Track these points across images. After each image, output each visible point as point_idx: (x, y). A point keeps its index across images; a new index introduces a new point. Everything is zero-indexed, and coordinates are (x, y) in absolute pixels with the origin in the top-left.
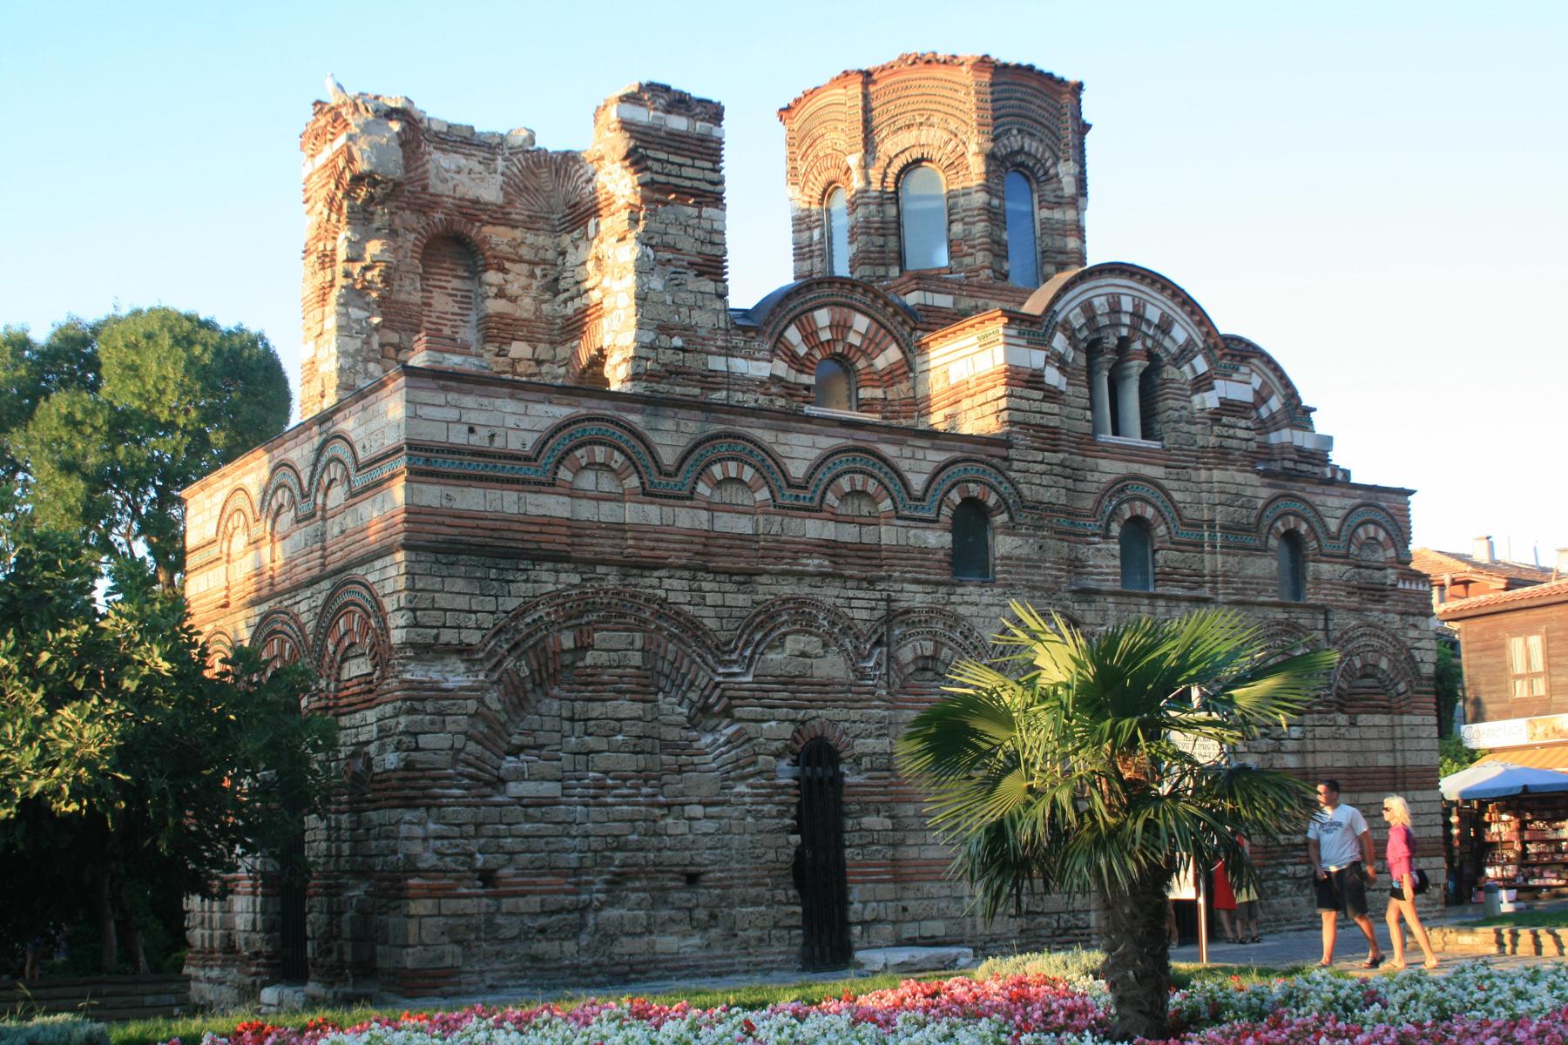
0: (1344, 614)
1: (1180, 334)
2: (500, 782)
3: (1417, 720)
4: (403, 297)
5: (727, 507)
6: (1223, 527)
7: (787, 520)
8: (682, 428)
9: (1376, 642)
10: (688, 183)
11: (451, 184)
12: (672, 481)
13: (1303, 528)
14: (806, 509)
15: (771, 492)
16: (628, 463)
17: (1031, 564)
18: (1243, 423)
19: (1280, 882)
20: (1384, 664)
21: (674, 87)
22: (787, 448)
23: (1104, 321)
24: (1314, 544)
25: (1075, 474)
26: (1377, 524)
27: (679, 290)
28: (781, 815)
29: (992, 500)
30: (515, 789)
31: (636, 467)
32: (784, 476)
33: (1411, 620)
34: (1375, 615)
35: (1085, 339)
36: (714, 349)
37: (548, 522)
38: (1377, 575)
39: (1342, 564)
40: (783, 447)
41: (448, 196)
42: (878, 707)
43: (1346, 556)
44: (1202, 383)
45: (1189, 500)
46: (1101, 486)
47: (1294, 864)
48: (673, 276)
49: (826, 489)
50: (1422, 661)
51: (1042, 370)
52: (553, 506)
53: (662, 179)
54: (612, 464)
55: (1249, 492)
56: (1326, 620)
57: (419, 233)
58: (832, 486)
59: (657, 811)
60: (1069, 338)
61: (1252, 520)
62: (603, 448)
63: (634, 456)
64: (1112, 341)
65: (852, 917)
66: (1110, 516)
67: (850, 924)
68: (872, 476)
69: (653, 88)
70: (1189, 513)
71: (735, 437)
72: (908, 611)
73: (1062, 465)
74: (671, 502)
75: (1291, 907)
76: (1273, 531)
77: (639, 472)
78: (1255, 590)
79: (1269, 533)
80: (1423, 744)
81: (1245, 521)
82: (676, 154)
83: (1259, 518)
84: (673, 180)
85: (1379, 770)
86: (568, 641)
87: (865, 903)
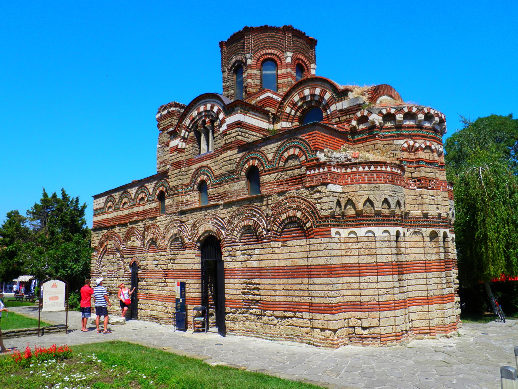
0: (277, 196)
1: (215, 109)
2: (100, 273)
3: (318, 241)
6: (224, 174)
9: (294, 205)
10: (166, 125)
13: (256, 163)
14: (134, 205)
17: (171, 206)
18: (234, 130)
19: (250, 315)
20: (299, 214)
23: (198, 118)
24: (262, 168)
25: (186, 173)
26: (295, 147)
28: (129, 280)
29: (164, 190)
30: (103, 274)
33: (315, 189)
34: (293, 192)
35: (192, 127)
37: (105, 220)
38: (296, 171)
39: (276, 172)
42: (143, 253)
43: (277, 168)
44: (223, 121)
45: (217, 168)
46: (192, 174)
47: (256, 309)
50: (322, 209)
51: (178, 145)
52: (105, 217)
53: (162, 127)
55: (234, 157)
56: (267, 200)
59: (116, 279)
60: (186, 131)
61: (235, 168)
64: (200, 122)
65: (138, 307)
66: (195, 182)
67: (138, 309)
68: (144, 192)
69: (161, 107)
70: (217, 173)
72: (149, 227)
73: (180, 172)
75: (255, 327)
76: (243, 170)
78: (236, 195)
79: (241, 171)
80: (321, 253)
81: (232, 169)
83: (237, 167)
85: (299, 267)
86: (105, 244)
87: (140, 304)
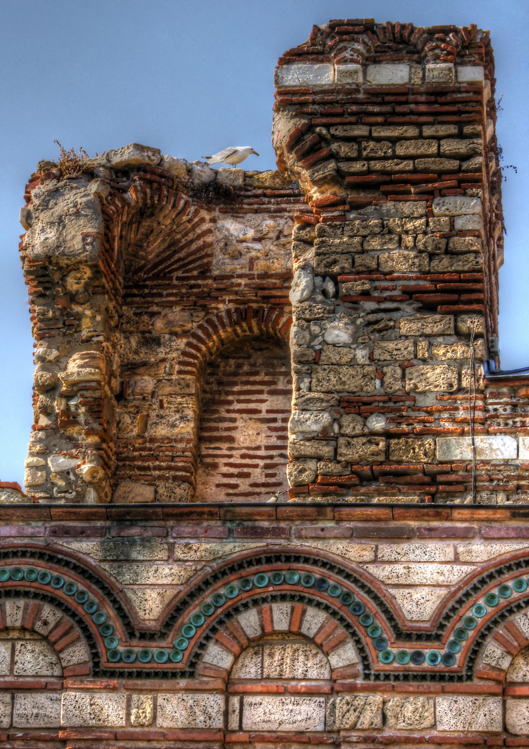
4: (162, 431)
5: (272, 686)
7: (394, 700)
8: (179, 554)
10: (408, 165)
11: (244, 261)
12: (154, 647)
15: (361, 650)
16: (68, 620)
21: (381, 20)
22: (399, 569)
27: (383, 339)
31: (85, 629)
32: (391, 619)
36: (448, 426)
40: (388, 568)
41: (240, 276)
48: (372, 317)
49: (483, 636)
53: (358, 166)
54: (38, 626)
57: (195, 336)
58: (500, 630)
62: (21, 603)
63: (80, 610)
71: (288, 559)
74: (148, 683)
77: (89, 637)
82: (385, 124)
84: (378, 166)
